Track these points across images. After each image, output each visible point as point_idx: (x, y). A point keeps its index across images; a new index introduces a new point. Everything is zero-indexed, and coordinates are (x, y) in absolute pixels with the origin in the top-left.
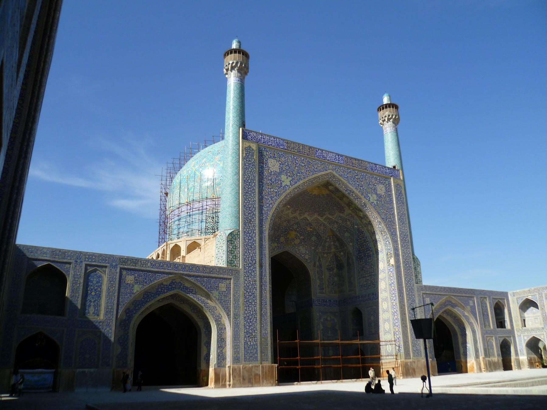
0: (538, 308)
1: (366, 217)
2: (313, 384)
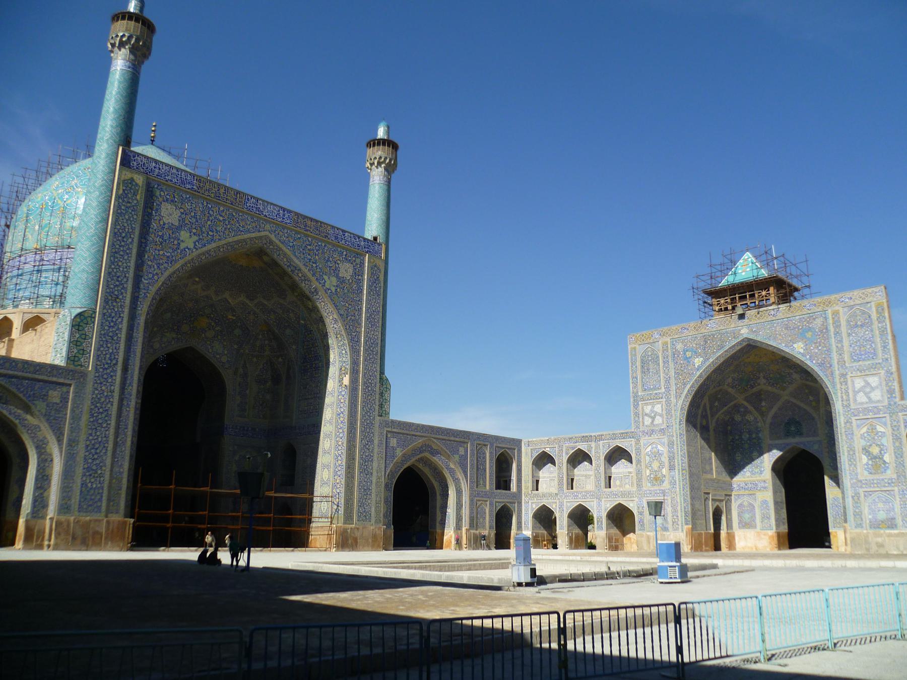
0: (591, 464)
1: (315, 309)
2: (191, 551)
